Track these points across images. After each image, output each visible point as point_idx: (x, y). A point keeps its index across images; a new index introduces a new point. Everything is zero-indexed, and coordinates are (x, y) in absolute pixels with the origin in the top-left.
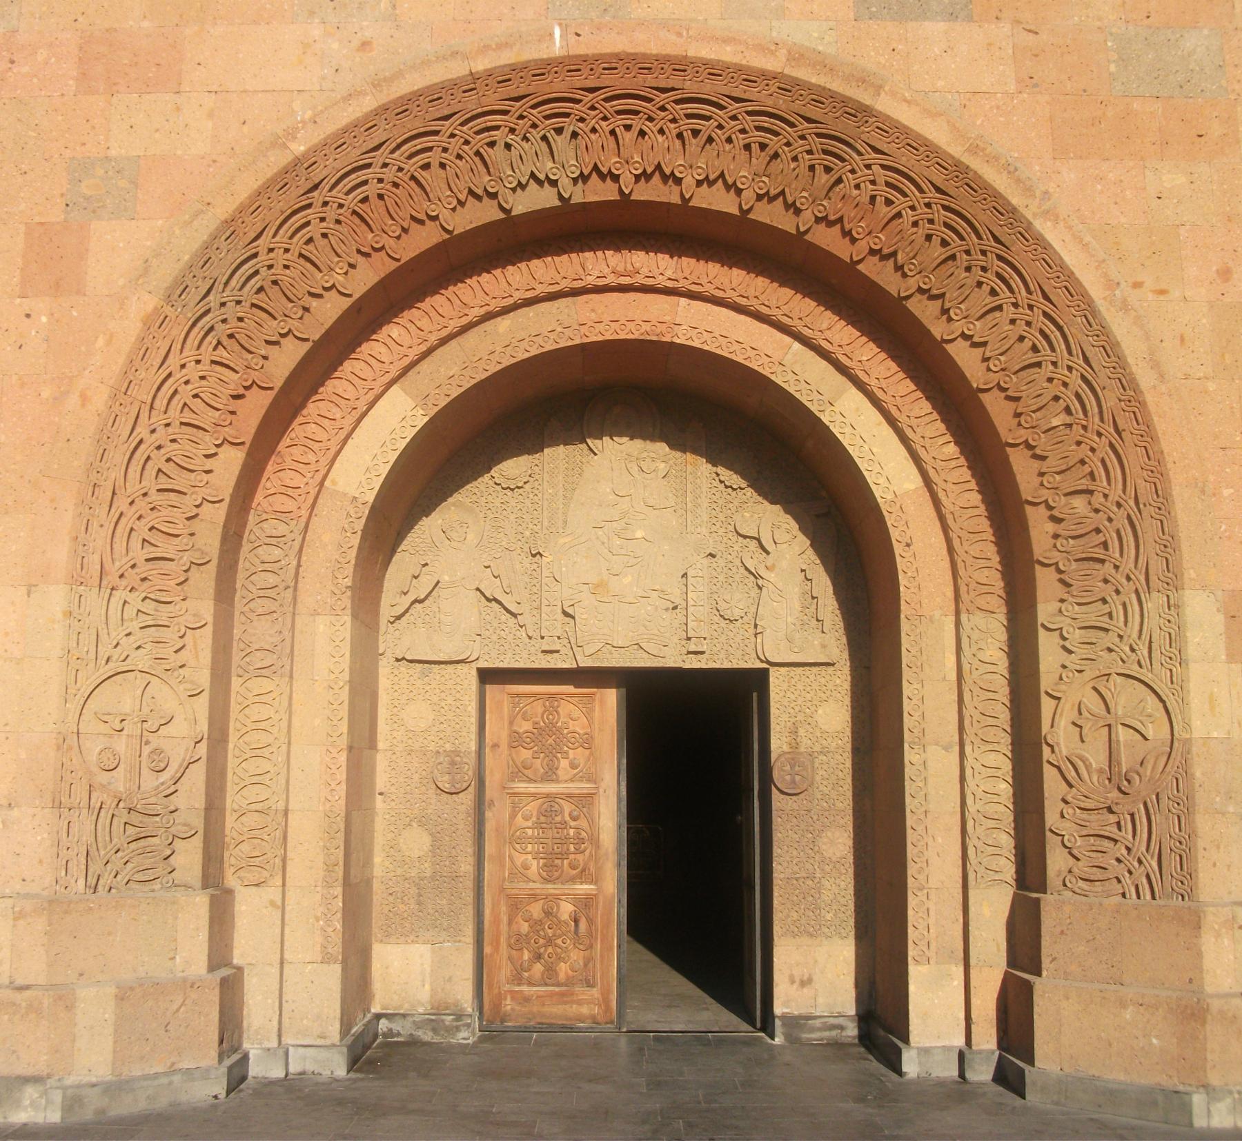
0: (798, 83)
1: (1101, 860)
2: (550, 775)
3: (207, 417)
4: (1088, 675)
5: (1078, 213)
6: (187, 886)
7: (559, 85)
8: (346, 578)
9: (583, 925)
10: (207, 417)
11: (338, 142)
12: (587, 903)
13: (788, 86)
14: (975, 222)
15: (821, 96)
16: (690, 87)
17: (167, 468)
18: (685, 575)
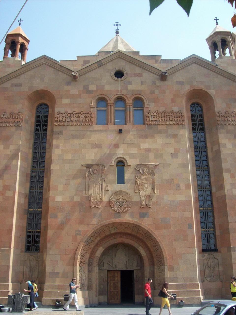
0: (135, 224)
1: (160, 287)
2: (114, 280)
3: (87, 252)
4: (158, 272)
5: (157, 235)
6: (86, 290)
7: (115, 224)
8: (97, 263)
9: (117, 294)
10: (87, 252)
11: (97, 229)
12: (117, 292)
13: (134, 224)
14: (149, 235)
15: (137, 225)
16: (126, 224)
17: (84, 256)
18: (126, 262)
